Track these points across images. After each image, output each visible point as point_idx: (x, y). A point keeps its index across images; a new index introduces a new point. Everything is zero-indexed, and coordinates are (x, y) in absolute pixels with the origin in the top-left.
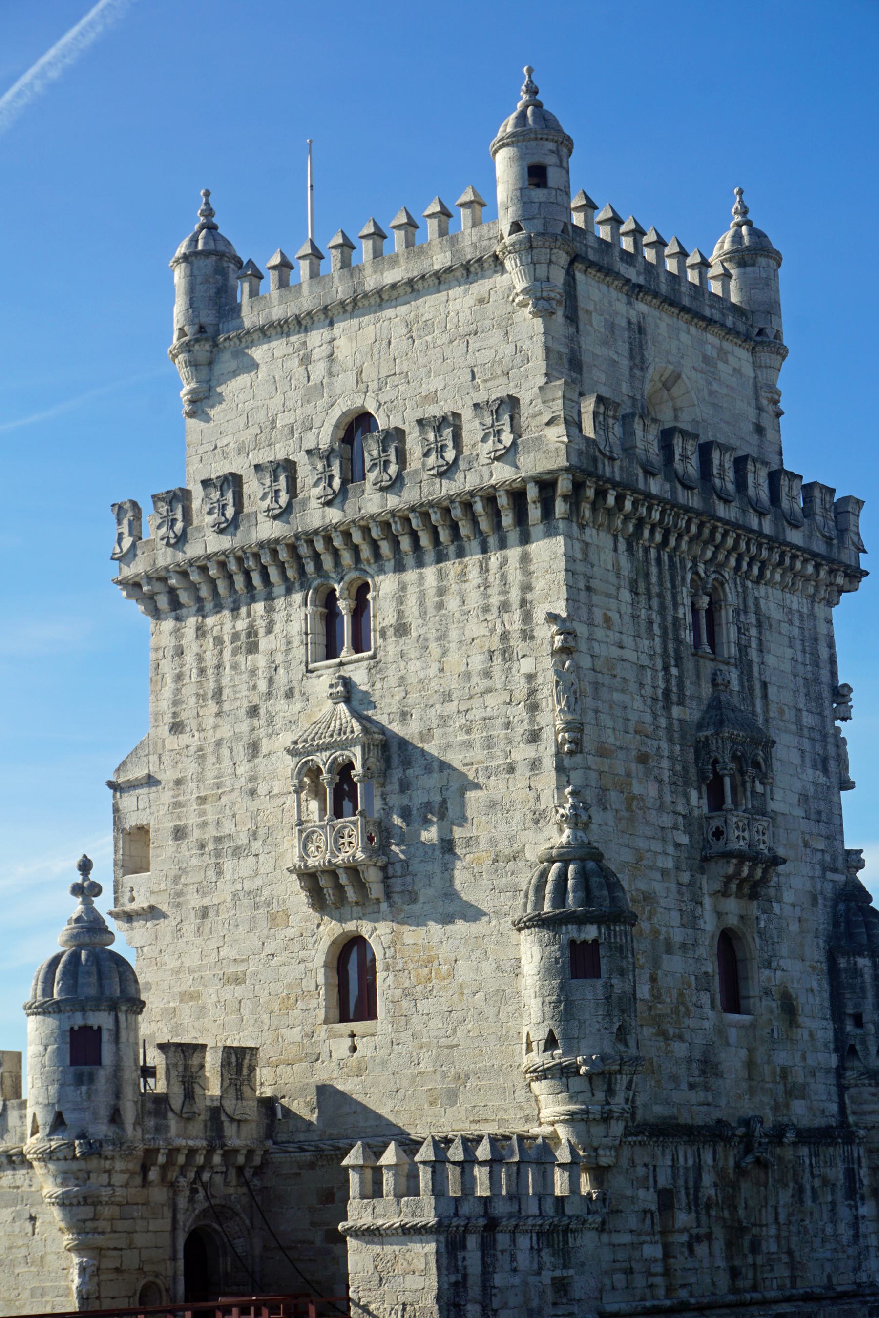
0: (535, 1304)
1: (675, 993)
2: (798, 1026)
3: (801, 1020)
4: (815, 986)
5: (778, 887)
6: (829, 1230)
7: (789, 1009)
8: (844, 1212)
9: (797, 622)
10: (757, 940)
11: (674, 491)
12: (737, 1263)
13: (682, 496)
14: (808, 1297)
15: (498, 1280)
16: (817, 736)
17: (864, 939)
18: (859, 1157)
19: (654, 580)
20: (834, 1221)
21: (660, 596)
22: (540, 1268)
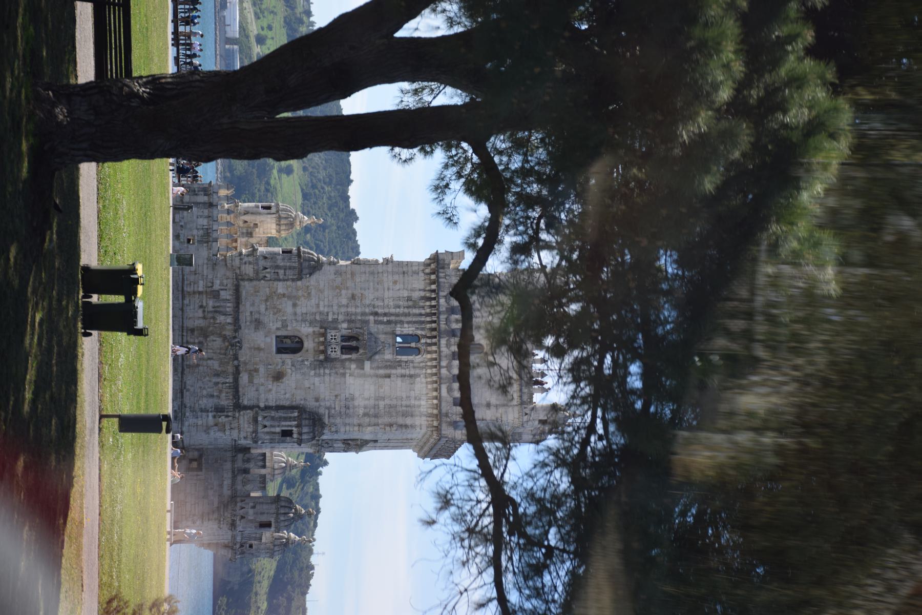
0: (188, 226)
1: (280, 307)
2: (273, 381)
4: (287, 396)
5: (319, 375)
6: (205, 392)
7: (278, 377)
9: (417, 403)
10: (300, 359)
11: (443, 313)
12: (196, 333)
13: (443, 317)
14: (182, 373)
17: (304, 416)
21: (409, 315)
22: (198, 229)
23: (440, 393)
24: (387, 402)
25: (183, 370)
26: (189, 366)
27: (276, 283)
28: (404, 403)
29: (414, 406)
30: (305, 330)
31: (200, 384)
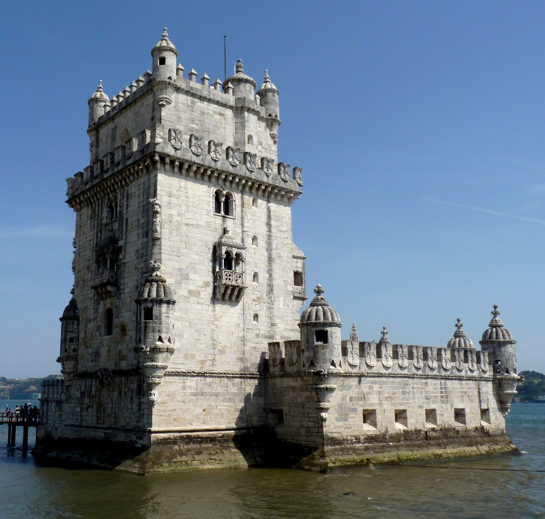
1: (90, 334)
2: (126, 335)
3: (127, 333)
4: (134, 319)
5: (124, 289)
6: (129, 406)
7: (123, 329)
8: (135, 400)
9: (142, 187)
15: (49, 413)
16: (145, 225)
18: (144, 380)
19: (97, 211)
20: (132, 403)
23: (129, 165)
24: (140, 217)
25: (115, 429)
26: (115, 422)
27: (80, 340)
28: (141, 199)
29: (143, 188)
30: (101, 309)
31: (125, 410)
